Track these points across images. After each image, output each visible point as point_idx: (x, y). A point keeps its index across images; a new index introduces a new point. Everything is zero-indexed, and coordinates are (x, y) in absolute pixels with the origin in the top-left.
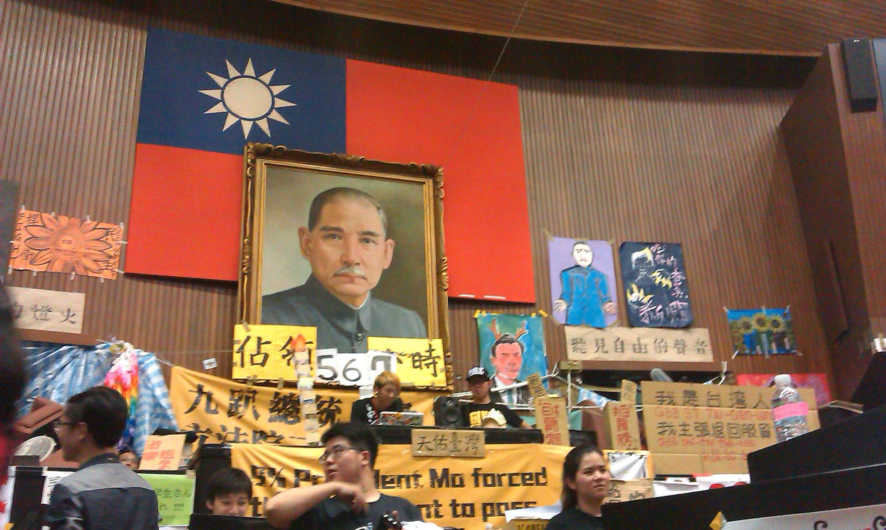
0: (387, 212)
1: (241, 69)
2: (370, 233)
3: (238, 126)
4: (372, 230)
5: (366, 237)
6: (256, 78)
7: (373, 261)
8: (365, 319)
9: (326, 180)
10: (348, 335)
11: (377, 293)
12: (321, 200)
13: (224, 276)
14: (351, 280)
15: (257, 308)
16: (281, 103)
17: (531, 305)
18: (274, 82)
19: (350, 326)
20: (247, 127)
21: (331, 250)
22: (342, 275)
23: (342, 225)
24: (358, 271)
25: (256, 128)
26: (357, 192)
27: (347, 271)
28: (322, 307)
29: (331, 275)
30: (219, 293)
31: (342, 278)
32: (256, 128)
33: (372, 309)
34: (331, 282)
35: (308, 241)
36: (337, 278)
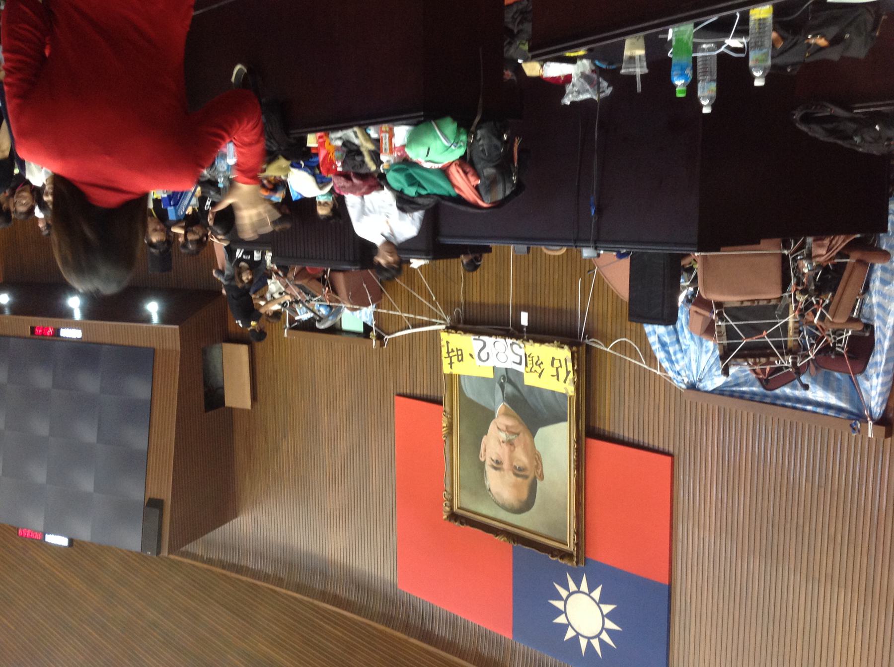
0: (484, 486)
1: (590, 646)
2: (496, 468)
3: (591, 588)
4: (494, 471)
5: (498, 465)
6: (578, 634)
7: (493, 443)
8: (499, 395)
9: (525, 522)
10: (510, 381)
12: (526, 505)
13: (596, 445)
14: (507, 427)
15: (571, 410)
16: (559, 604)
17: (400, 395)
21: (522, 458)
22: (514, 433)
23: (514, 477)
24: (503, 436)
25: (578, 585)
27: (511, 437)
29: (521, 434)
30: (604, 430)
31: (513, 430)
32: (578, 585)
33: (494, 402)
34: (521, 428)
35: (537, 467)
36: (518, 431)
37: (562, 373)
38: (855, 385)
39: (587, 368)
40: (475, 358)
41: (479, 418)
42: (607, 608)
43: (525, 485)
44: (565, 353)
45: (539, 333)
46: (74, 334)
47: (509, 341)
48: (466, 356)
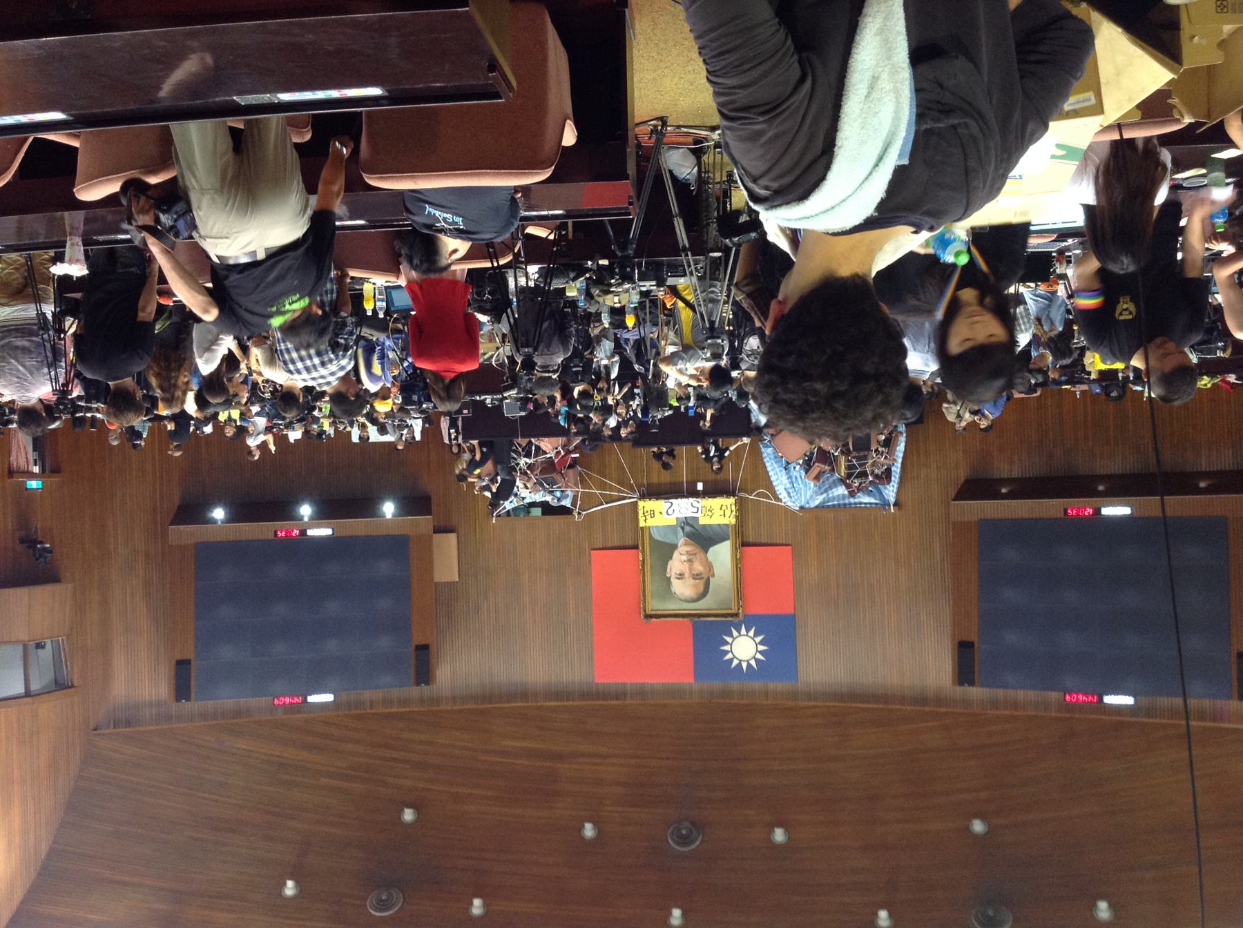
3: (748, 631)
5: (681, 576)
7: (677, 564)
8: (680, 533)
10: (688, 524)
11: (675, 547)
13: (746, 549)
18: (731, 661)
19: (688, 529)
20: (743, 631)
21: (698, 567)
24: (684, 558)
25: (739, 632)
26: (687, 601)
28: (703, 538)
32: (739, 632)
37: (728, 512)
38: (880, 493)
39: (741, 506)
40: (660, 515)
41: (665, 551)
42: (758, 639)
43: (701, 584)
44: (732, 500)
45: (710, 492)
46: (327, 532)
47: (691, 500)
48: (657, 513)
